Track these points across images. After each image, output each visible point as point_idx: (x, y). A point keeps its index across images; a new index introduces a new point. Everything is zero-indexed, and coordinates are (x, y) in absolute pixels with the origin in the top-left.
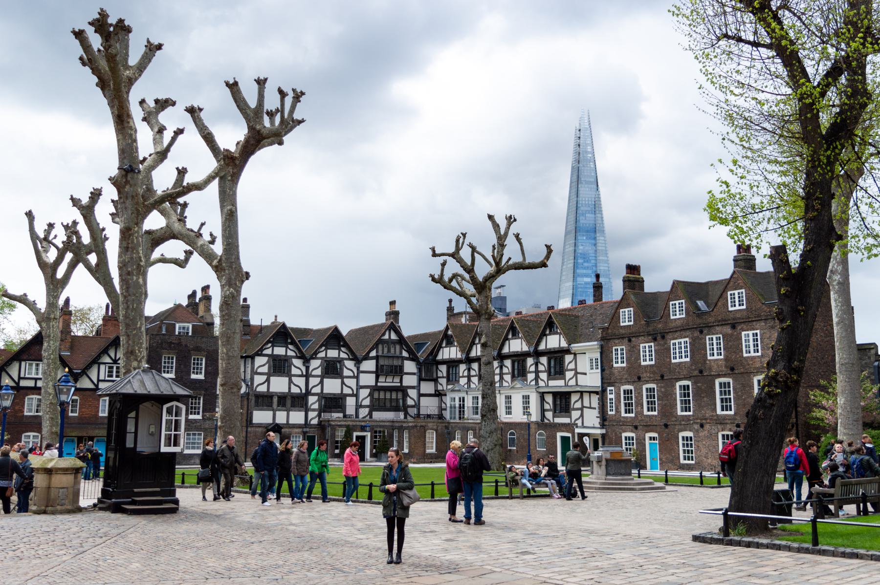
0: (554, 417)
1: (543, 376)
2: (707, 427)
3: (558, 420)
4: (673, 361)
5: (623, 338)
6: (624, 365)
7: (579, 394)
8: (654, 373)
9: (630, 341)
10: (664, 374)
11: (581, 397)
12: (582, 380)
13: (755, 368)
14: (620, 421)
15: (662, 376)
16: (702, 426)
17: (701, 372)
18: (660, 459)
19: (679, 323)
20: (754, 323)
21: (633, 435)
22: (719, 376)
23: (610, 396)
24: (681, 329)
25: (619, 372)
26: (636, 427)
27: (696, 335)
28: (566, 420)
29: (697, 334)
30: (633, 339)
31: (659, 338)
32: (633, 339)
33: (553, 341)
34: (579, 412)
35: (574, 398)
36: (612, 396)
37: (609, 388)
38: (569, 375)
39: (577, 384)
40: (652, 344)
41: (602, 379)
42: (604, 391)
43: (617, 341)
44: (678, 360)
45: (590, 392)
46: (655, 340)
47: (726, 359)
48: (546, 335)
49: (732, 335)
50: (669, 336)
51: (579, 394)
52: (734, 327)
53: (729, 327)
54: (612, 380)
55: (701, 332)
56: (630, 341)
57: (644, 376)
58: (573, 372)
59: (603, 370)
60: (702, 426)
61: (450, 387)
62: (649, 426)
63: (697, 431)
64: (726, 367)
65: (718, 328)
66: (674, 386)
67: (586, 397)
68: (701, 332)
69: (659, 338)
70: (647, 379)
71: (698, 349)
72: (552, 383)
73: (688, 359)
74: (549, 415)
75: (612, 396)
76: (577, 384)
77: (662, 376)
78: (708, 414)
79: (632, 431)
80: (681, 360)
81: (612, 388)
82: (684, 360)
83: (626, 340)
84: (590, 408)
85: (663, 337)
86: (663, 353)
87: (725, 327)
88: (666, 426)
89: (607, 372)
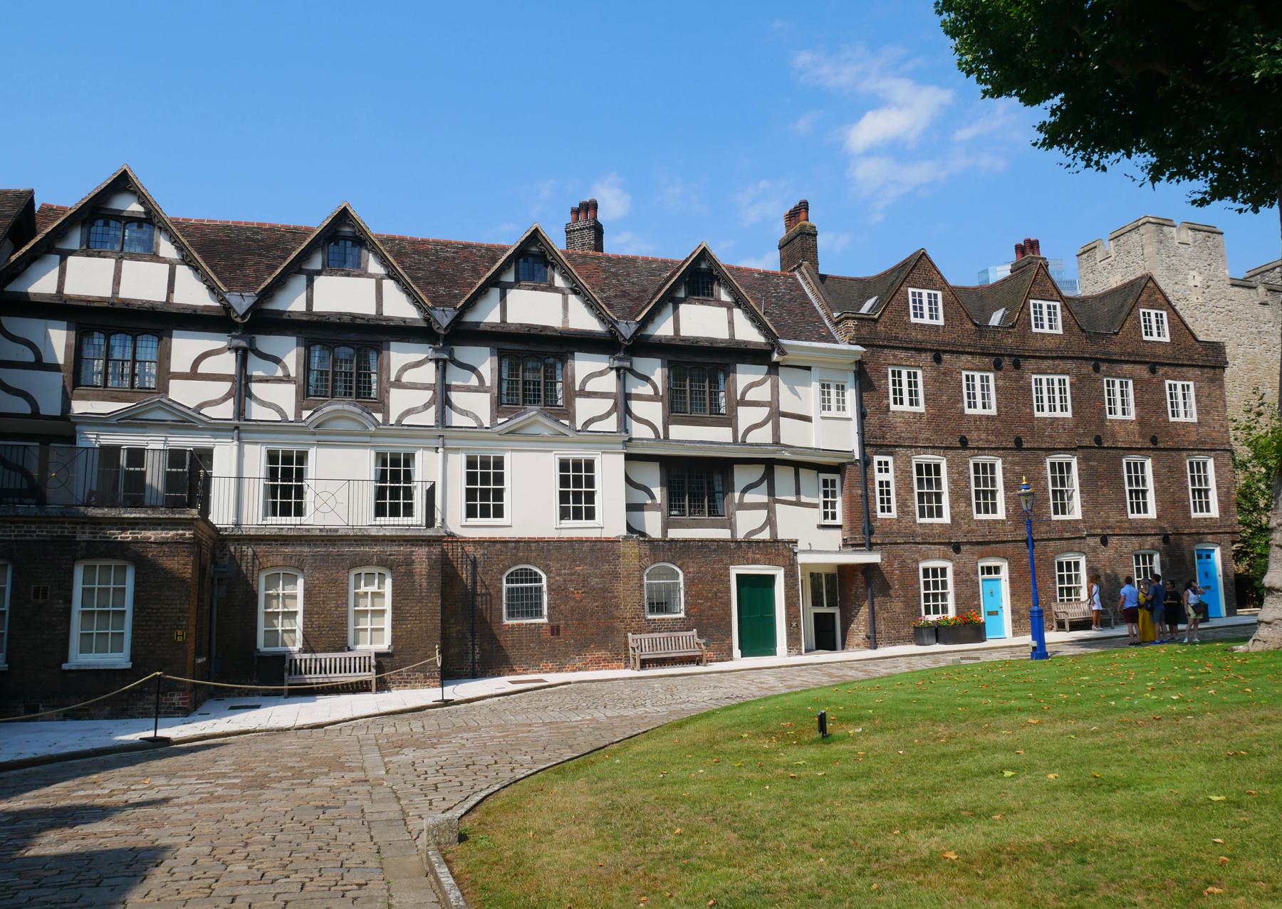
0: (666, 526)
1: (653, 411)
2: (1113, 541)
3: (674, 534)
4: (1037, 414)
5: (919, 350)
6: (921, 408)
7: (759, 471)
8: (998, 433)
9: (938, 359)
10: (1019, 438)
11: (769, 477)
12: (792, 434)
13: (1191, 443)
14: (914, 534)
15: (1018, 442)
16: (1104, 541)
17: (1098, 440)
18: (1013, 612)
19: (1051, 344)
20: (1184, 369)
21: (949, 566)
22: (1130, 450)
23: (879, 477)
24: (1053, 356)
25: (908, 423)
26: (957, 548)
27: (1084, 371)
28: (724, 534)
29: (1087, 368)
30: (946, 357)
31: (1007, 362)
32: (946, 357)
33: (702, 321)
34: (762, 515)
35: (742, 477)
36: (889, 477)
37: (877, 458)
38: (746, 416)
39: (777, 442)
40: (991, 376)
41: (862, 434)
42: (867, 463)
43: (902, 354)
44: (1046, 414)
45: (797, 465)
46: (997, 367)
47: (1141, 421)
48: (676, 303)
49: (1149, 381)
50: (1029, 364)
51: (759, 471)
52: (1153, 371)
53: (1145, 367)
54: (890, 439)
55: (1096, 369)
56: (938, 359)
57: (974, 437)
58: (764, 412)
59: (862, 415)
60: (1104, 541)
61: (79, 407)
62: (988, 543)
63: (1094, 550)
64: (1142, 435)
65: (1127, 367)
66: (1042, 463)
67: (783, 477)
68: (1096, 369)
69: (1007, 362)
70: (981, 444)
71: (1088, 401)
72: (679, 432)
73: (1069, 414)
74: (653, 523)
75: (889, 477)
76: (777, 442)
77: (1018, 442)
78: (1113, 518)
79: (945, 558)
80: (1053, 414)
81: (890, 459)
82: (1058, 414)
83: (927, 358)
84: (798, 504)
85: (1017, 366)
86: (1016, 397)
87: (1138, 367)
88: (1030, 542)
89: (872, 420)
